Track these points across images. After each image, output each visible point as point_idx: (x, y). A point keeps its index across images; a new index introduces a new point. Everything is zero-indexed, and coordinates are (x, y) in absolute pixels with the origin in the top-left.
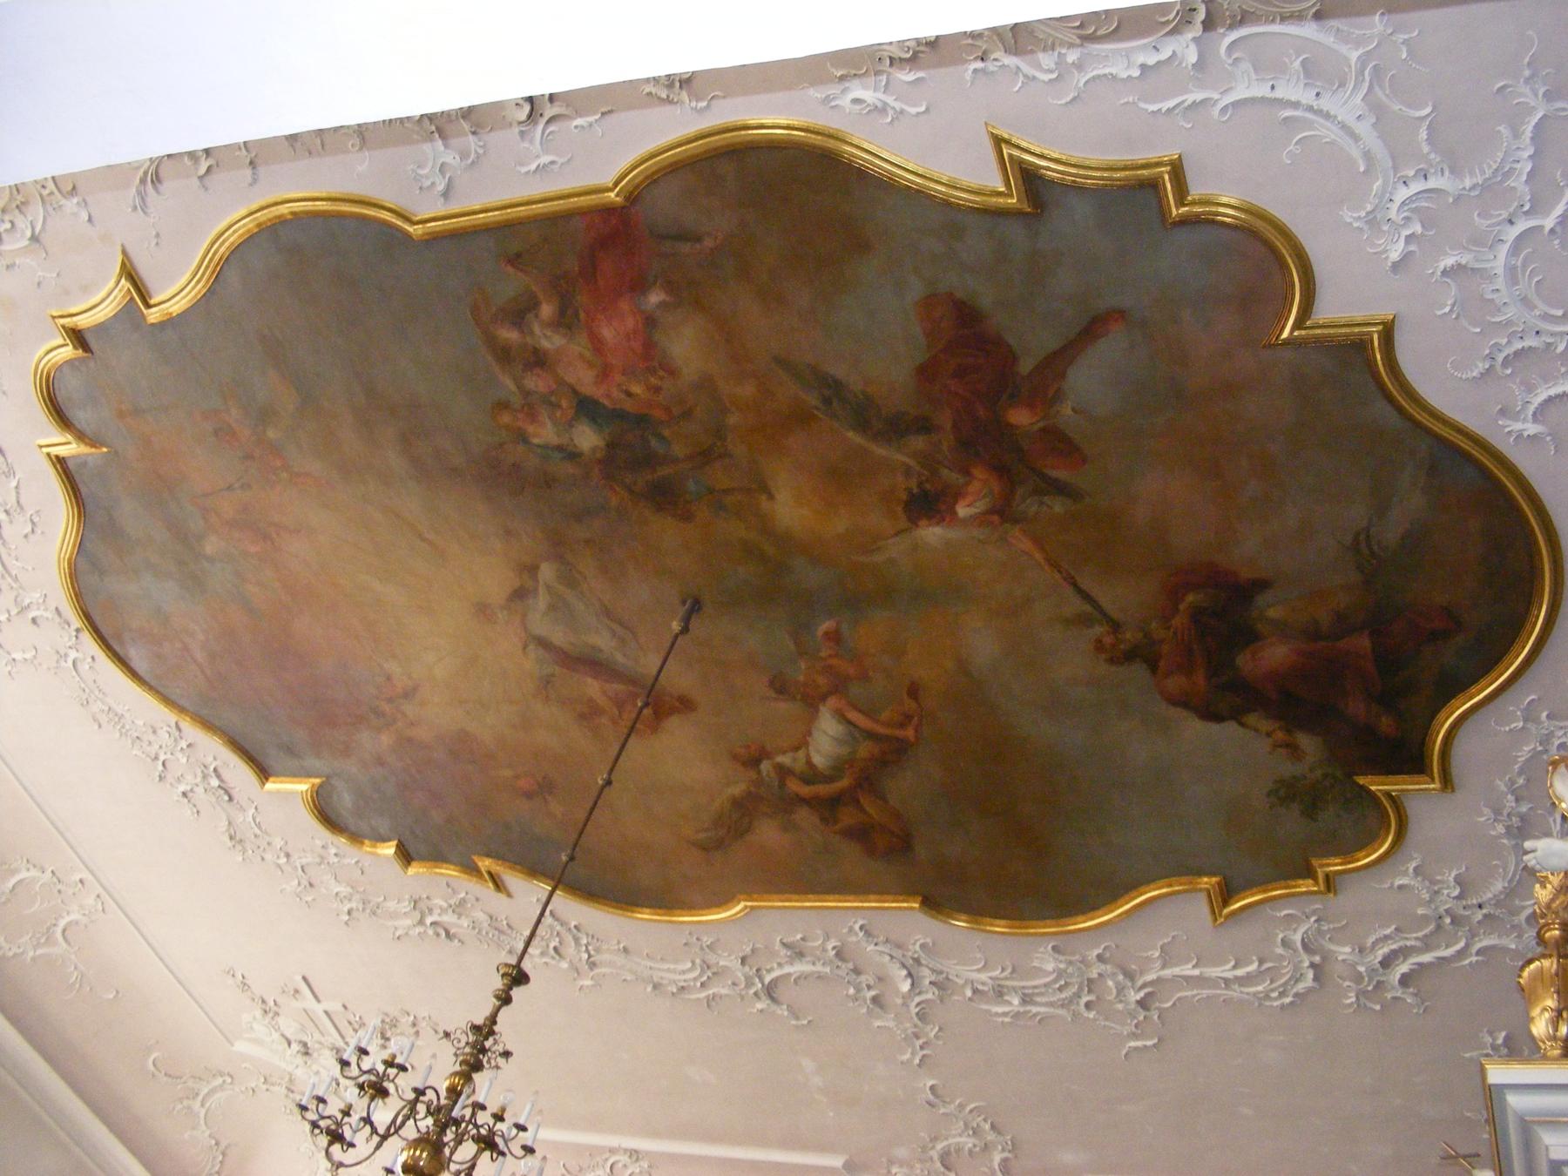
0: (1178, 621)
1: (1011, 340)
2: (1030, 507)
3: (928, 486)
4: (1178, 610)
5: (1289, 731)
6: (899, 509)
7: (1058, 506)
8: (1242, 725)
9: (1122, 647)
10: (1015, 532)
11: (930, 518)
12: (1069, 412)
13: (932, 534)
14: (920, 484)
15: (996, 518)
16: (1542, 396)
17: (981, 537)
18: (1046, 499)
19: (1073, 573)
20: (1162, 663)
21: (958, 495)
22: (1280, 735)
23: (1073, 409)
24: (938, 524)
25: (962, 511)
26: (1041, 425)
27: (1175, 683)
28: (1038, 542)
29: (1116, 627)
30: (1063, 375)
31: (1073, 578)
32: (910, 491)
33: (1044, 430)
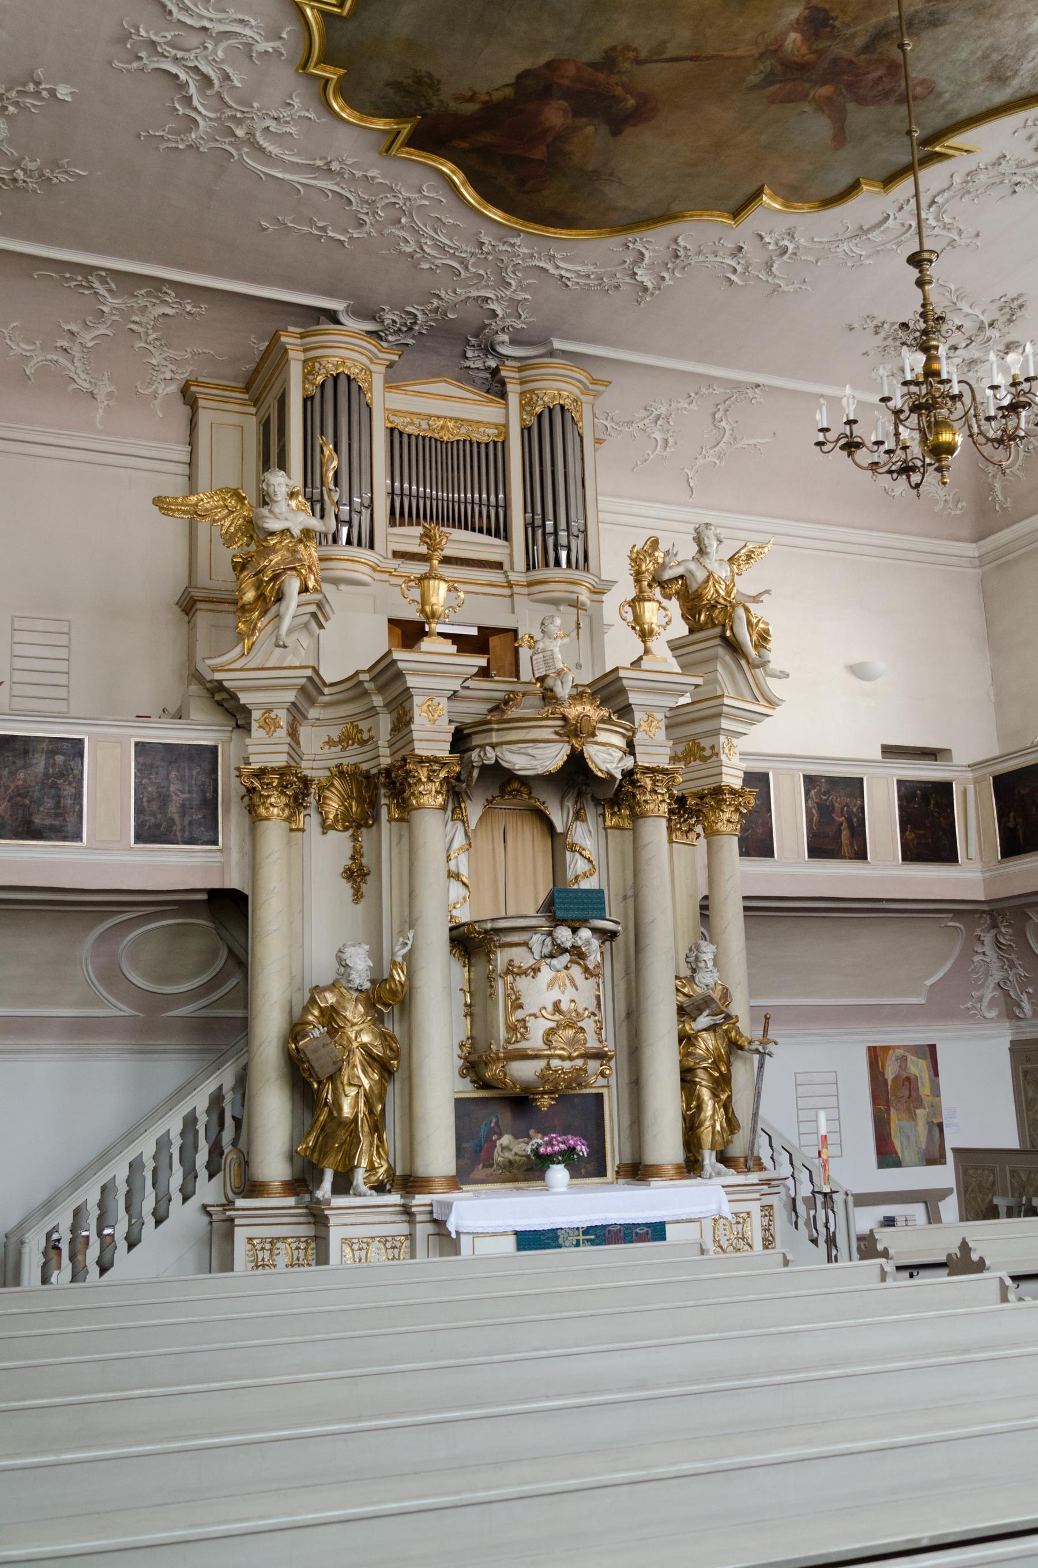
0: (619, 91)
1: (872, 108)
2: (765, 66)
3: (828, 29)
4: (627, 93)
5: (485, 103)
6: (827, 6)
7: (753, 79)
8: (507, 85)
9: (620, 58)
10: (756, 52)
11: (806, 17)
12: (806, 109)
13: (794, 13)
14: (833, 27)
15: (774, 48)
16: (647, 254)
17: (766, 35)
18: (762, 76)
19: (699, 62)
20: (590, 70)
21: (806, 39)
22: (485, 98)
23: (805, 112)
24: (798, 20)
25: (794, 36)
26: (811, 95)
27: (571, 70)
28: (741, 58)
29: (639, 62)
30: (829, 117)
31: (695, 61)
32: (835, 19)
33: (807, 95)
